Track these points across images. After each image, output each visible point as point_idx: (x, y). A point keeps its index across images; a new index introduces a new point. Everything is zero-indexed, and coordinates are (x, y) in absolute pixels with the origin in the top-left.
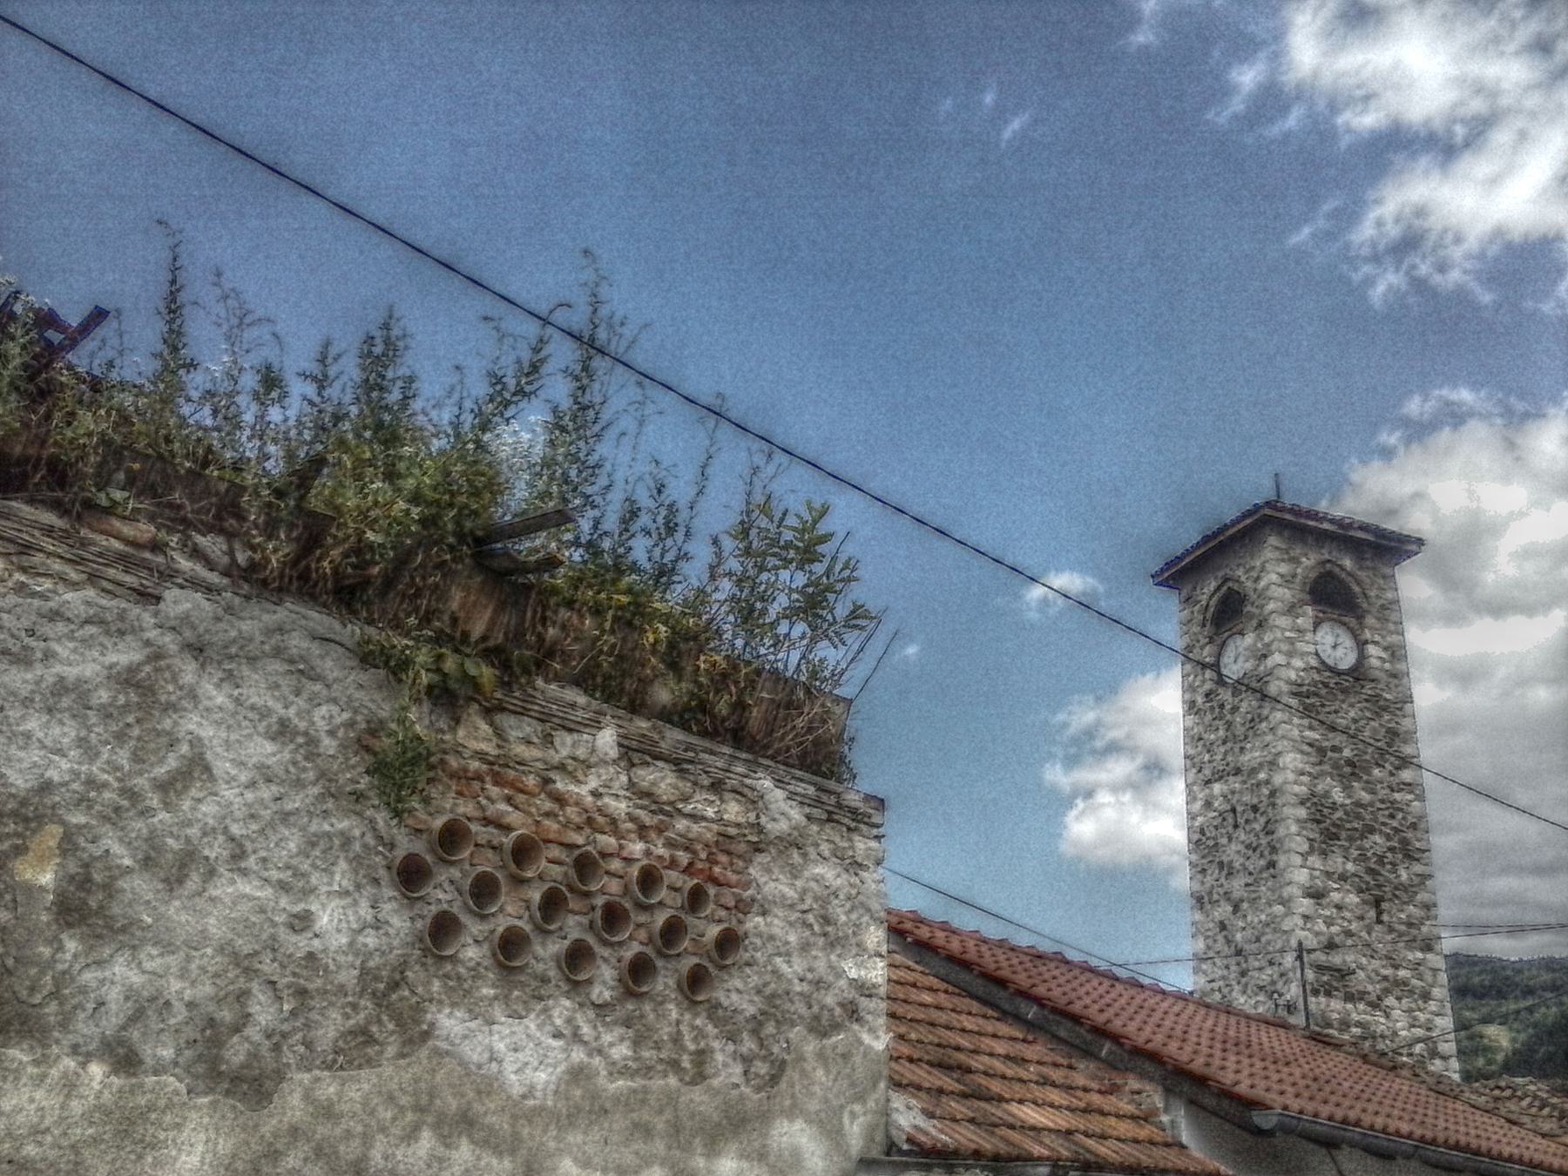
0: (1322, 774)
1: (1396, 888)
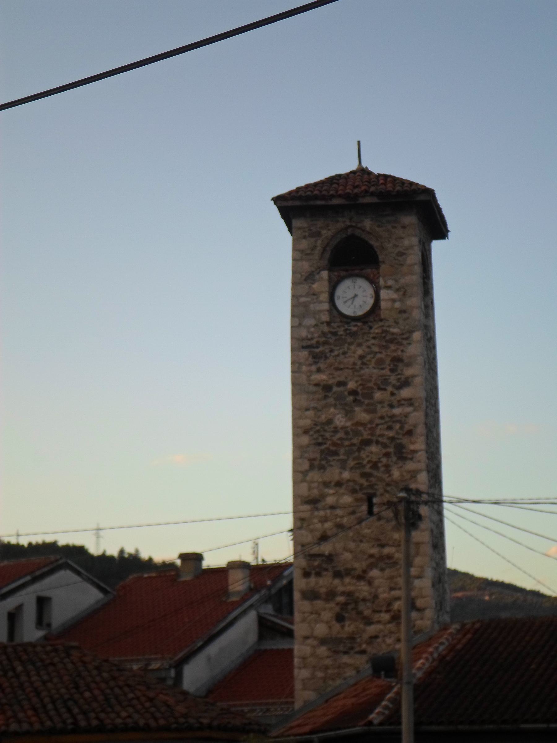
0: (327, 406)
1: (388, 485)
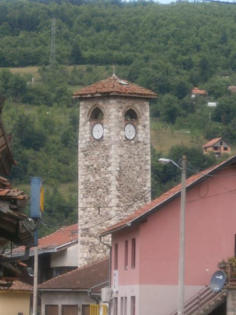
1: (104, 204)
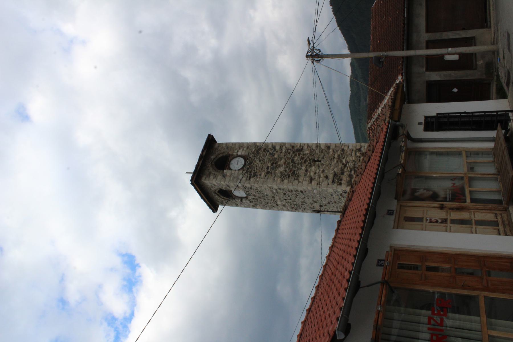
0: (275, 173)
1: (311, 155)
